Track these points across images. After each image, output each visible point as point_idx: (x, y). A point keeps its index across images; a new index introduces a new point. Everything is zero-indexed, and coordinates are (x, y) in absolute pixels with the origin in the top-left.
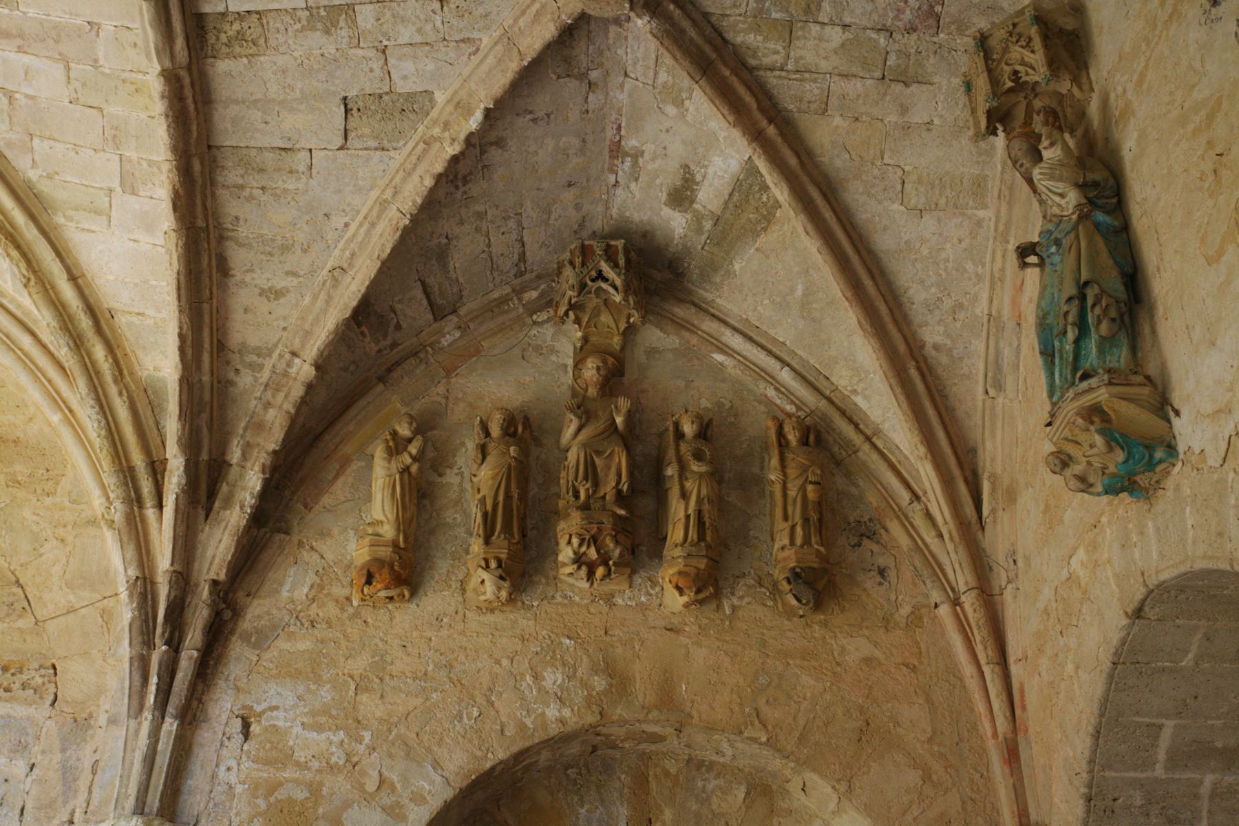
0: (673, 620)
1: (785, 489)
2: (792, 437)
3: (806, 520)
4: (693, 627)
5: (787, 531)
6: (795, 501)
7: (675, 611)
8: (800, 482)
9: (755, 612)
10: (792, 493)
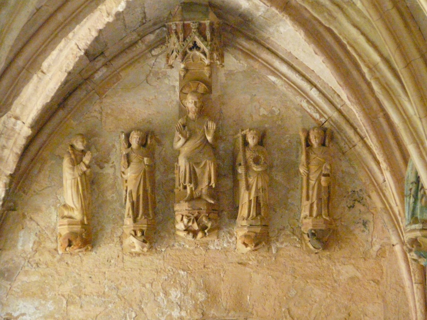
0: (242, 258)
1: (308, 179)
2: (315, 142)
3: (319, 199)
4: (254, 262)
5: (308, 207)
6: (313, 187)
7: (243, 252)
8: (317, 175)
9: (290, 251)
10: (312, 182)
